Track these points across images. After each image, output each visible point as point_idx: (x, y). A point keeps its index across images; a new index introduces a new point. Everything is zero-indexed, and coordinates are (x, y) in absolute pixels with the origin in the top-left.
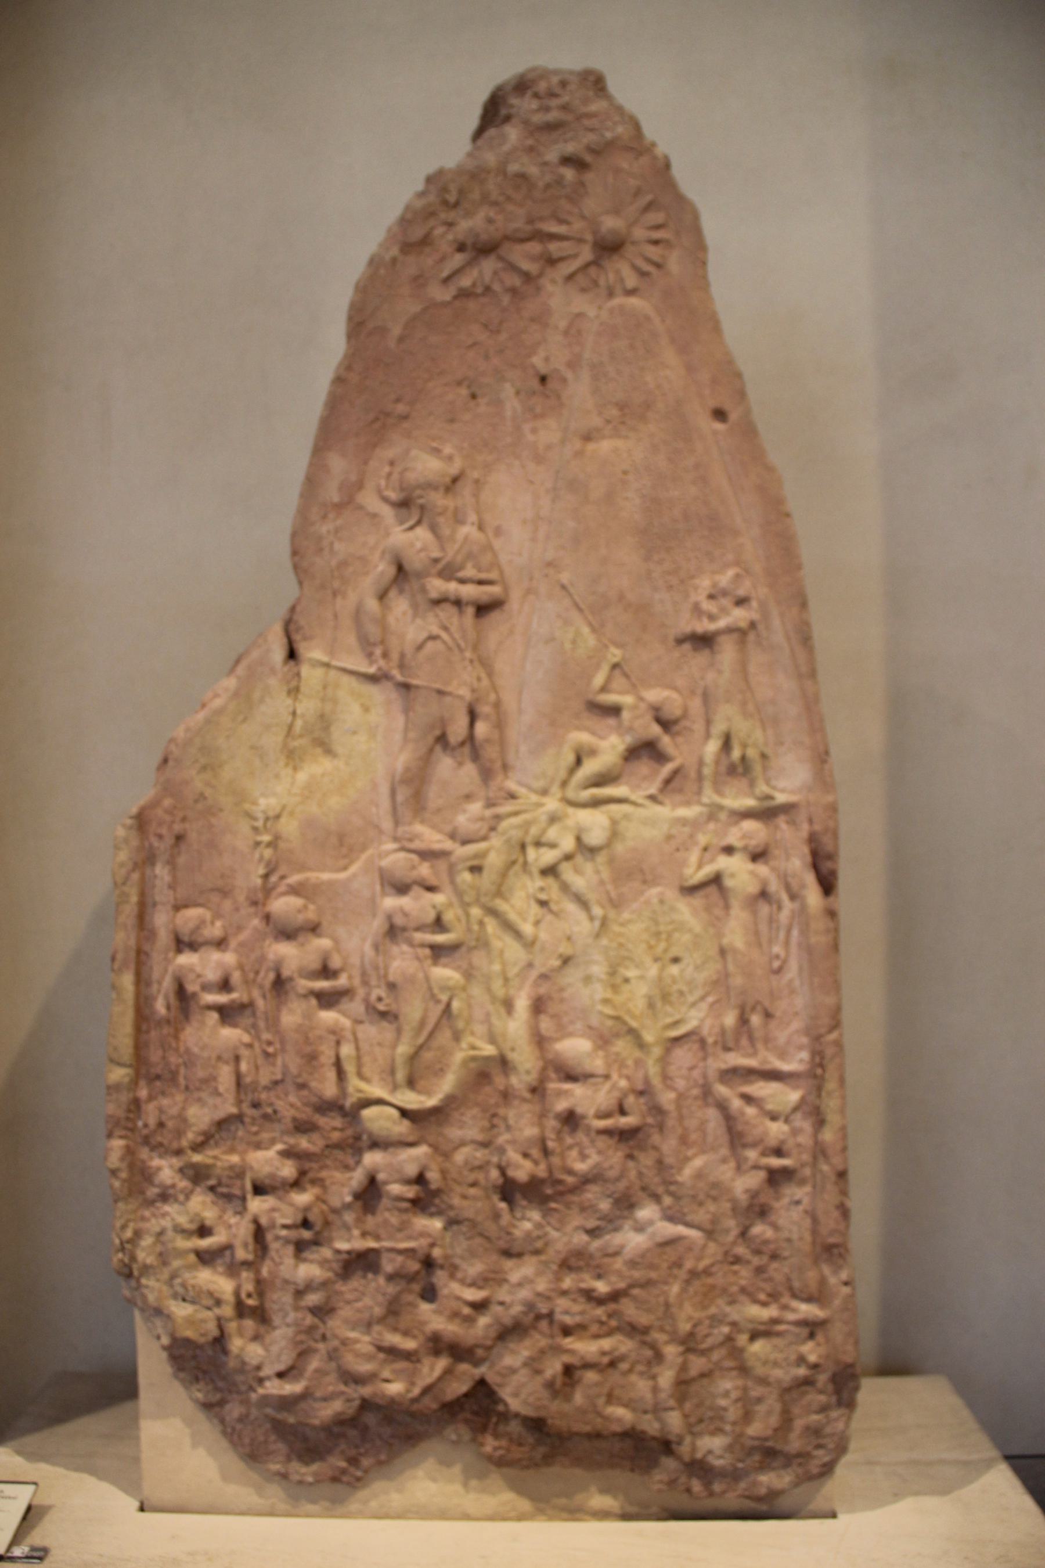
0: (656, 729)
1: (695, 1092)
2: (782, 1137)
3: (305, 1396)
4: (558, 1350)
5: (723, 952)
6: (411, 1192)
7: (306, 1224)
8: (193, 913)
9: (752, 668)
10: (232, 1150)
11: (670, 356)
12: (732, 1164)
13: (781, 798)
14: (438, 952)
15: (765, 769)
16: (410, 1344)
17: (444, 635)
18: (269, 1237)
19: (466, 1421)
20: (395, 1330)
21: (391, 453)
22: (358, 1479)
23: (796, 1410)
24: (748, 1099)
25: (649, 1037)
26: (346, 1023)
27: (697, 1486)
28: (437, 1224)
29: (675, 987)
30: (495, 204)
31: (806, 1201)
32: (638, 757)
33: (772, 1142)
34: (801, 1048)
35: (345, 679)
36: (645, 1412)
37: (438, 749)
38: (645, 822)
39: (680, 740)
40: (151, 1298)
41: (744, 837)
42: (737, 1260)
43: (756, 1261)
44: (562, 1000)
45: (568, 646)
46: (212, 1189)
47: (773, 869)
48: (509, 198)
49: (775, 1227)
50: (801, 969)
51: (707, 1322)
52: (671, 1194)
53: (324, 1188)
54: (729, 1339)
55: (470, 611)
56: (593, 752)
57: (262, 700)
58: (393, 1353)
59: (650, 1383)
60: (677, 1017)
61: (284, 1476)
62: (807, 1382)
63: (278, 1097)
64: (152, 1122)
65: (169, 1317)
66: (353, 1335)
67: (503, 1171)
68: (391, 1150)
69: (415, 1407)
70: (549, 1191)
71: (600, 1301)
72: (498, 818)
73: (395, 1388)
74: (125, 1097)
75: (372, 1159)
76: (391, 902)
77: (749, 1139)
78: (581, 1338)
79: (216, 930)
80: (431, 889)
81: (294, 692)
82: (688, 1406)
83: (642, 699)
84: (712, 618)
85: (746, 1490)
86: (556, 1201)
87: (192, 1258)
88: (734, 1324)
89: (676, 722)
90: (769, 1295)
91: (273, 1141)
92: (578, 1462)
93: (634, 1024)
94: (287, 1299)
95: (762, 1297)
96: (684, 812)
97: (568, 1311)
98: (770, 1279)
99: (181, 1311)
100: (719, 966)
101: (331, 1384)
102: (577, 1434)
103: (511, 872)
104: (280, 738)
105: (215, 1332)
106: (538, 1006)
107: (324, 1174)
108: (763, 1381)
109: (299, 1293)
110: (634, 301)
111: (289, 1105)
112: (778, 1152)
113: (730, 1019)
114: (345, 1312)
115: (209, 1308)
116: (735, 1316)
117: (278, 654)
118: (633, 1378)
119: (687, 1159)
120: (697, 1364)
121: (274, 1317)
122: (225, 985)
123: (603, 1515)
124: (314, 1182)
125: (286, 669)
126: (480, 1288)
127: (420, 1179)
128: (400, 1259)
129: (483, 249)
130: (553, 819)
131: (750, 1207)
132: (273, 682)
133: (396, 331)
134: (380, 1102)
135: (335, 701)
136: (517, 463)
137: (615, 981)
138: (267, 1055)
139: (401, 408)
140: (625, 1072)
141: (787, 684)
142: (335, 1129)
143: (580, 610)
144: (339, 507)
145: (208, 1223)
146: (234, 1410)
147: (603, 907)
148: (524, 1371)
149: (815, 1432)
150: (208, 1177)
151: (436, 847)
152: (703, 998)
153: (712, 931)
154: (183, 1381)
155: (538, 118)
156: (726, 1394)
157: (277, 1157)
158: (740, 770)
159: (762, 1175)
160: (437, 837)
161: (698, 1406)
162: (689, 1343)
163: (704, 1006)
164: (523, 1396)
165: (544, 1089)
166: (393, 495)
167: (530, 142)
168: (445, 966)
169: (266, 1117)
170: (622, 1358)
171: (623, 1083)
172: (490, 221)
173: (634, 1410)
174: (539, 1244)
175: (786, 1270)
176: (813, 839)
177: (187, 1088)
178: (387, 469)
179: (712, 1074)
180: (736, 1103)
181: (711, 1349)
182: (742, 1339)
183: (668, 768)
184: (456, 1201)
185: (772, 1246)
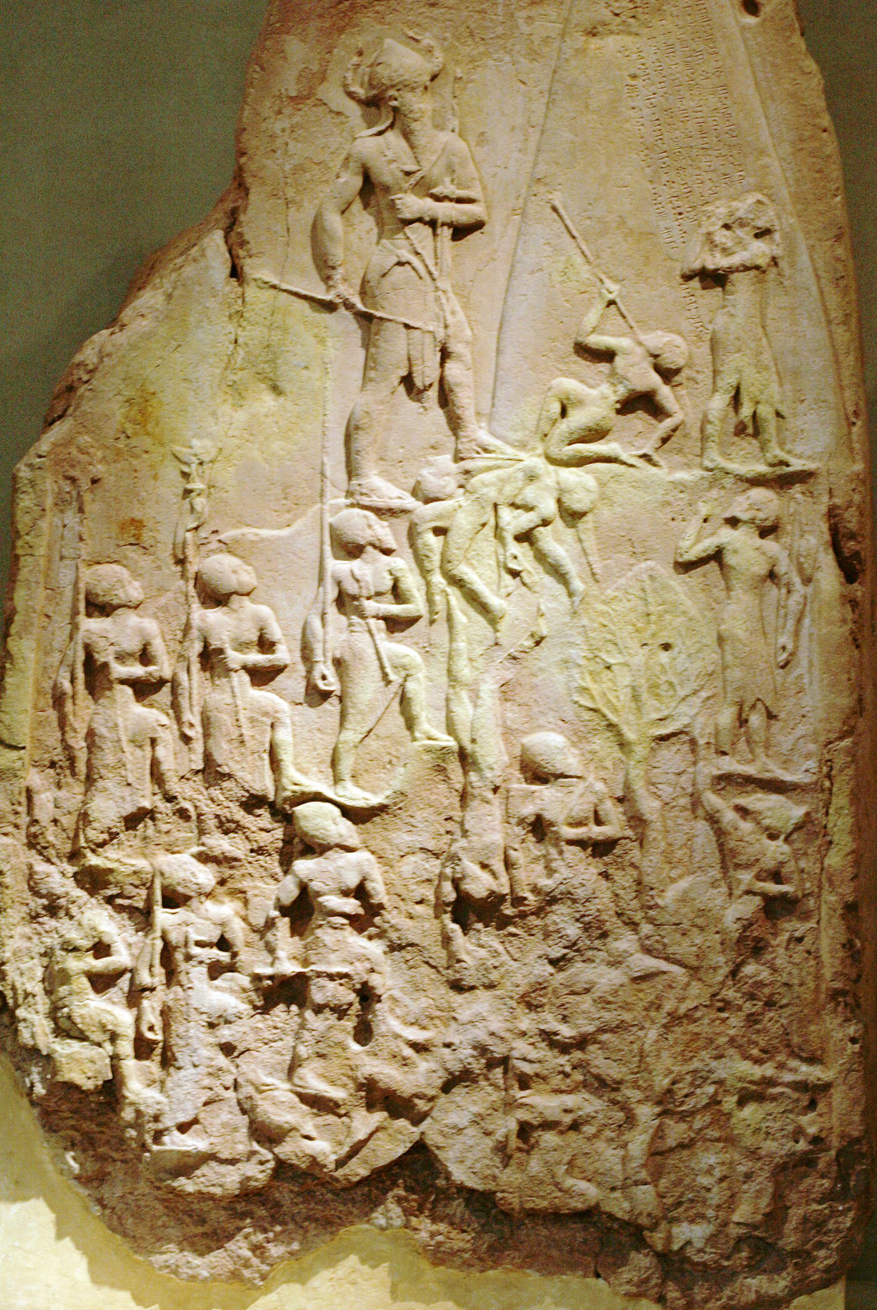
0: (655, 379)
2: (781, 858)
4: (510, 1105)
5: (721, 640)
7: (223, 944)
9: (771, 312)
12: (724, 889)
13: (797, 465)
14: (395, 624)
15: (779, 429)
16: (336, 1093)
18: (179, 956)
19: (399, 1200)
21: (360, 41)
23: (794, 1197)
24: (743, 811)
25: (630, 735)
28: (376, 948)
29: (664, 678)
32: (632, 411)
33: (769, 863)
34: (808, 756)
36: (613, 1189)
37: (402, 389)
38: (636, 484)
39: (682, 391)
41: (751, 507)
42: (726, 1006)
43: (748, 1007)
44: (534, 687)
46: (110, 900)
49: (774, 970)
50: (811, 664)
51: (689, 1078)
52: (651, 921)
53: (246, 902)
54: (714, 1101)
55: (447, 232)
56: (580, 403)
58: (318, 1104)
59: (622, 1152)
60: (665, 713)
62: (807, 1161)
65: (49, 1057)
66: (269, 1080)
67: (456, 883)
68: (329, 854)
69: (339, 1174)
70: (508, 910)
71: (564, 1048)
75: (303, 866)
77: (742, 859)
78: (539, 1092)
79: (134, 591)
80: (387, 552)
82: (663, 1182)
83: (640, 344)
84: (726, 251)
85: (730, 1298)
86: (515, 925)
87: (85, 982)
88: (720, 1083)
89: (677, 371)
90: (764, 1051)
91: (187, 844)
93: (614, 719)
98: (765, 1031)
100: (716, 657)
101: (242, 1144)
102: (533, 1214)
103: (480, 535)
104: (218, 371)
106: (506, 691)
107: (245, 884)
108: (753, 1154)
112: (776, 876)
113: (726, 717)
115: (99, 1045)
116: (721, 1074)
118: (600, 1145)
119: (673, 880)
120: (676, 1131)
121: (178, 1055)
125: (228, 288)
126: (424, 1028)
127: (360, 892)
128: (331, 985)
130: (532, 477)
131: (741, 940)
132: (211, 303)
134: (318, 797)
135: (285, 330)
136: (507, 58)
138: (186, 739)
140: (602, 774)
142: (262, 830)
145: (106, 940)
147: (585, 583)
148: (471, 1131)
150: (106, 884)
151: (395, 504)
152: (695, 692)
153: (709, 615)
156: (709, 1171)
157: (194, 861)
158: (750, 430)
159: (757, 900)
160: (397, 492)
161: (676, 1184)
162: (667, 1103)
163: (697, 701)
164: (468, 1163)
165: (508, 791)
166: (361, 92)
168: (399, 642)
169: (183, 814)
170: (588, 1120)
171: (599, 786)
173: (599, 1184)
174: (494, 976)
175: (784, 1021)
176: (832, 514)
178: (356, 59)
179: (703, 781)
181: (692, 1113)
182: (730, 1102)
183: (668, 423)
185: (767, 991)
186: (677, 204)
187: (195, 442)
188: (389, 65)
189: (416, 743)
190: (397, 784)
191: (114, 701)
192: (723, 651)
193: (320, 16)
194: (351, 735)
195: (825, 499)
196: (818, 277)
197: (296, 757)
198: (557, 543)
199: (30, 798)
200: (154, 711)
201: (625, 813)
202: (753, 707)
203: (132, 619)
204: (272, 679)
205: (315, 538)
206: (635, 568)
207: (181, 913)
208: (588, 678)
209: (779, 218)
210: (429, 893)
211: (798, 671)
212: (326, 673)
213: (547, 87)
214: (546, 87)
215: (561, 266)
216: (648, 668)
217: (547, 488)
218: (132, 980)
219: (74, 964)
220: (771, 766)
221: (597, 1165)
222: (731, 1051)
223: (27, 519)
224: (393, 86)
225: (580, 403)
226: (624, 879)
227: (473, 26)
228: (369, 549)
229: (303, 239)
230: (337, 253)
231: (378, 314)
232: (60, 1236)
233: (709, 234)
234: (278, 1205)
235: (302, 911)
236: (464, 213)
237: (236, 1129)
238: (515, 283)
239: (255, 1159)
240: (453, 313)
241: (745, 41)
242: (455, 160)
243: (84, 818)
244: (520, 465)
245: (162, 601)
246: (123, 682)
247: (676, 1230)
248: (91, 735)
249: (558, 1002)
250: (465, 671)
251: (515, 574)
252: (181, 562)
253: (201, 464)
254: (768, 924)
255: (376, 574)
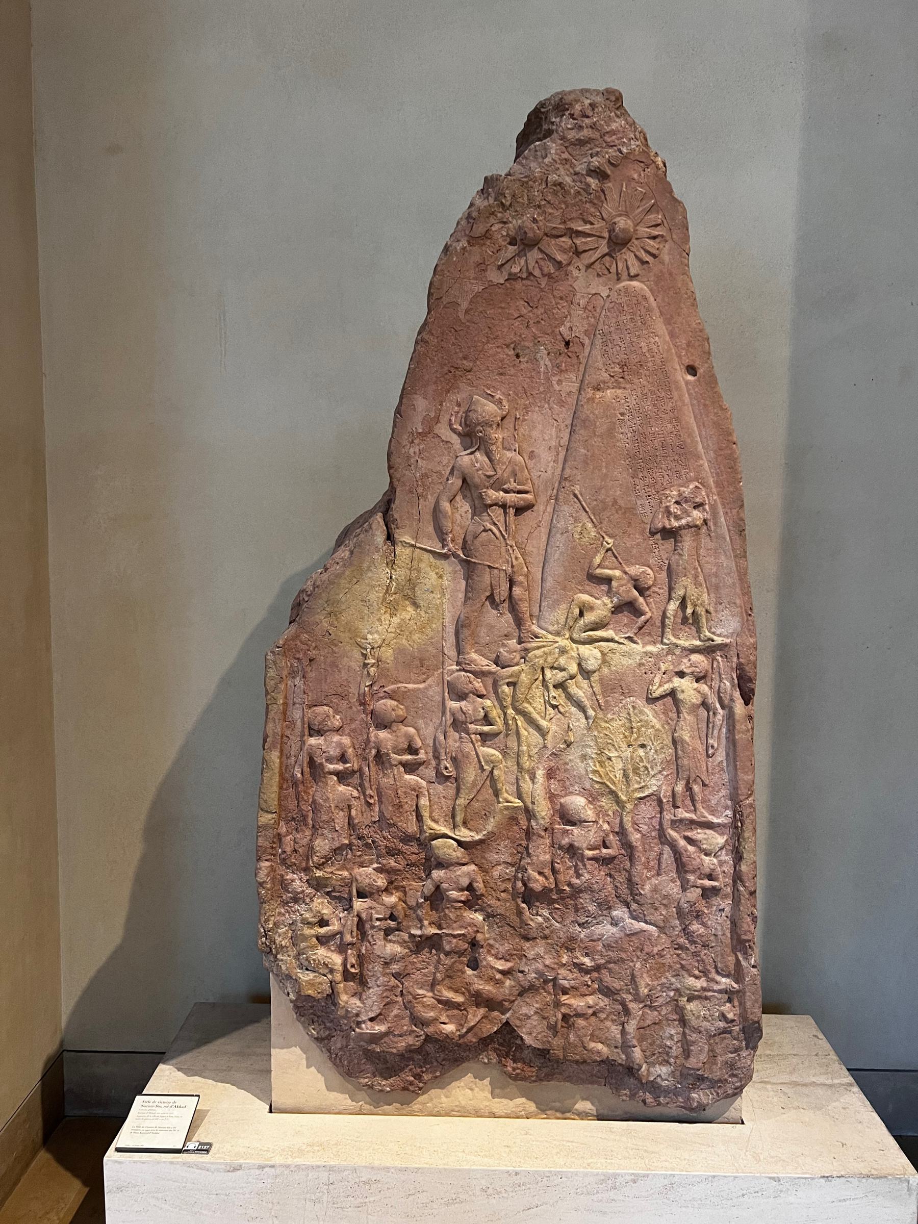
0: (636, 593)
1: (653, 834)
3: (386, 1034)
6: (464, 896)
7: (392, 917)
8: (319, 709)
9: (702, 552)
10: (343, 868)
11: (661, 327)
13: (718, 640)
14: (485, 738)
15: (707, 619)
16: (460, 999)
17: (495, 530)
18: (367, 926)
19: (495, 1050)
20: (450, 988)
22: (420, 1089)
24: (687, 839)
25: (624, 798)
26: (424, 783)
27: (649, 1099)
28: (479, 917)
30: (539, 206)
31: (727, 909)
34: (726, 808)
35: (426, 556)
37: (487, 603)
40: (284, 968)
41: (691, 666)
43: (693, 948)
45: (577, 536)
46: (328, 893)
47: (711, 687)
48: (549, 202)
51: (659, 988)
53: (405, 893)
55: (512, 511)
56: (592, 608)
57: (369, 569)
58: (448, 1004)
61: (371, 1087)
62: (725, 1031)
63: (376, 832)
64: (288, 849)
66: (421, 992)
68: (451, 868)
69: (461, 1041)
71: (587, 972)
72: (526, 650)
73: (450, 1028)
74: (270, 833)
75: (437, 874)
76: (454, 705)
78: (574, 996)
79: (337, 721)
80: (481, 696)
81: (392, 564)
83: (626, 573)
84: (677, 518)
92: (569, 1079)
94: (378, 968)
95: (697, 972)
96: (650, 648)
97: (567, 978)
99: (306, 977)
103: (534, 686)
105: (329, 991)
106: (551, 774)
109: (386, 964)
110: (635, 283)
111: (383, 839)
112: (710, 877)
114: (417, 976)
115: (325, 975)
117: (380, 537)
118: (608, 1023)
120: (652, 1016)
122: (343, 758)
123: (583, 1115)
124: (397, 888)
127: (470, 888)
128: (455, 941)
129: (524, 242)
130: (563, 651)
133: (464, 305)
135: (419, 570)
136: (546, 406)
137: (604, 760)
138: (369, 805)
139: (467, 364)
141: (727, 562)
143: (586, 512)
144: (423, 435)
145: (325, 917)
146: (337, 1043)
147: (595, 711)
148: (535, 1017)
149: (731, 1065)
154: (303, 1023)
155: (571, 135)
157: (373, 872)
159: (699, 891)
160: (485, 662)
164: (534, 1035)
165: (553, 829)
167: (566, 156)
168: (489, 747)
169: (367, 845)
170: (602, 1010)
172: (535, 221)
173: (608, 1046)
174: (547, 932)
176: (740, 667)
177: (313, 826)
180: (682, 843)
184: (492, 902)
186: (648, 490)
187: (369, 636)
188: (476, 411)
189: (500, 805)
190: (490, 828)
191: (327, 784)
192: (676, 748)
193: (435, 383)
194: (461, 801)
195: (735, 659)
196: (729, 531)
197: (431, 813)
198: (580, 688)
199: (280, 840)
200: (350, 788)
201: (620, 841)
202: (695, 780)
203: (336, 738)
204: (418, 769)
205: (438, 689)
206: (624, 702)
207: (368, 902)
208: (598, 765)
209: (708, 497)
210: (509, 886)
211: (720, 759)
212: (448, 765)
213: (570, 422)
214: (569, 422)
215: (579, 529)
216: (632, 759)
217: (572, 658)
218: (342, 939)
219: (307, 931)
220: (706, 814)
221: (607, 1035)
222: (684, 973)
223: (272, 682)
224: (479, 424)
225: (592, 608)
226: (621, 878)
227: (526, 386)
228: (471, 695)
229: (427, 517)
230: (447, 525)
231: (473, 560)
232: (308, 1067)
233: (667, 507)
234: (428, 1054)
235: (436, 898)
236: (522, 499)
237: (403, 1018)
238: (551, 539)
239: (414, 1035)
240: (516, 558)
241: (688, 390)
242: (517, 468)
243: (311, 849)
244: (557, 645)
245: (353, 726)
246: (331, 773)
247: (652, 1069)
248: (315, 805)
249: (583, 946)
250: (527, 764)
251: (554, 707)
252: (363, 704)
253: (373, 648)
254: (704, 902)
255: (475, 710)
